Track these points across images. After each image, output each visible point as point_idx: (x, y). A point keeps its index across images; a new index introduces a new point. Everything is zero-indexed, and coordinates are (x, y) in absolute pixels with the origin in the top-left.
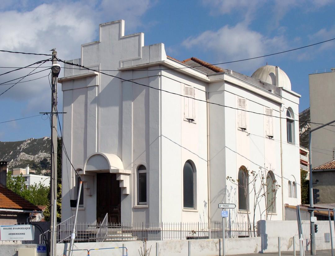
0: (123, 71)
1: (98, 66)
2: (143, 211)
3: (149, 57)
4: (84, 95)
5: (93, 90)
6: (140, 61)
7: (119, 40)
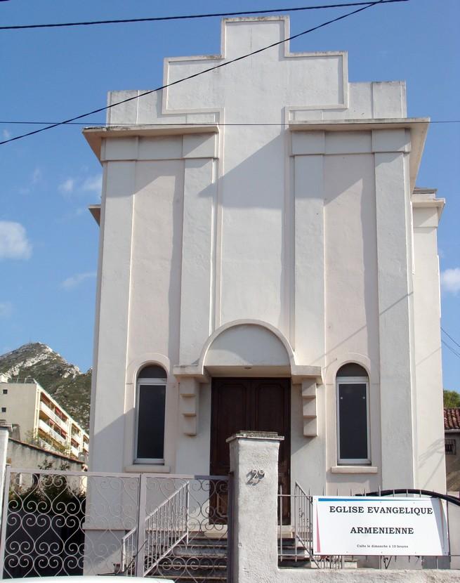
0: (299, 131)
1: (218, 114)
2: (362, 482)
3: (370, 108)
4: (173, 178)
5: (202, 169)
6: (344, 113)
7: (280, 60)
